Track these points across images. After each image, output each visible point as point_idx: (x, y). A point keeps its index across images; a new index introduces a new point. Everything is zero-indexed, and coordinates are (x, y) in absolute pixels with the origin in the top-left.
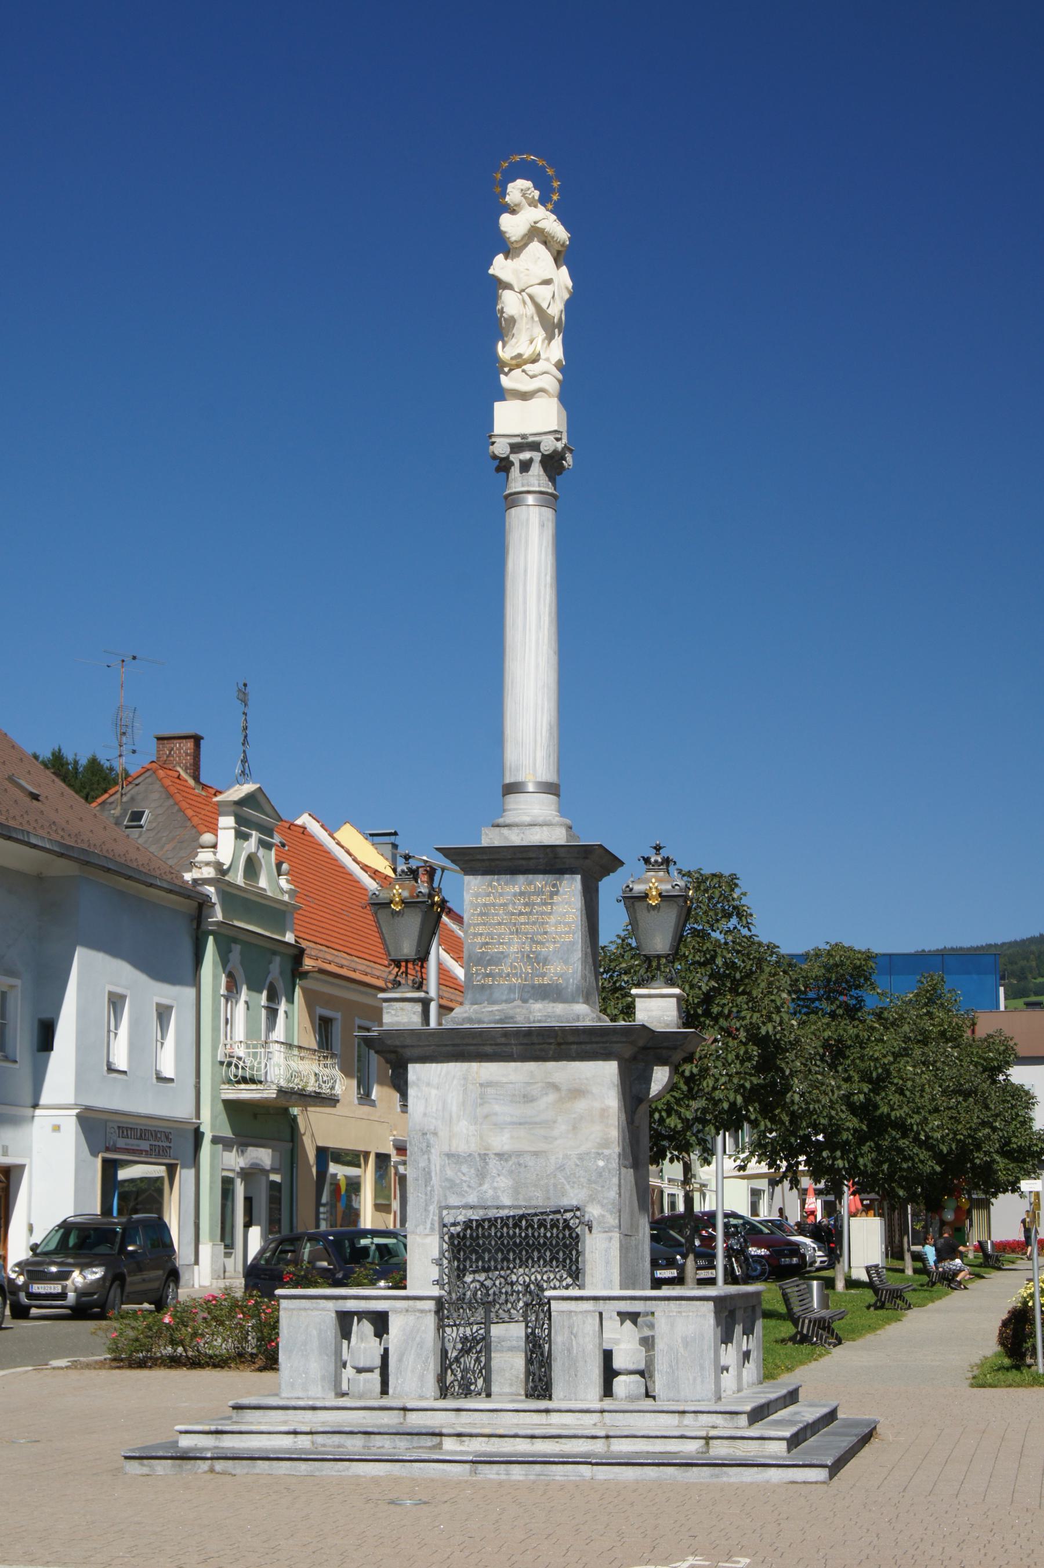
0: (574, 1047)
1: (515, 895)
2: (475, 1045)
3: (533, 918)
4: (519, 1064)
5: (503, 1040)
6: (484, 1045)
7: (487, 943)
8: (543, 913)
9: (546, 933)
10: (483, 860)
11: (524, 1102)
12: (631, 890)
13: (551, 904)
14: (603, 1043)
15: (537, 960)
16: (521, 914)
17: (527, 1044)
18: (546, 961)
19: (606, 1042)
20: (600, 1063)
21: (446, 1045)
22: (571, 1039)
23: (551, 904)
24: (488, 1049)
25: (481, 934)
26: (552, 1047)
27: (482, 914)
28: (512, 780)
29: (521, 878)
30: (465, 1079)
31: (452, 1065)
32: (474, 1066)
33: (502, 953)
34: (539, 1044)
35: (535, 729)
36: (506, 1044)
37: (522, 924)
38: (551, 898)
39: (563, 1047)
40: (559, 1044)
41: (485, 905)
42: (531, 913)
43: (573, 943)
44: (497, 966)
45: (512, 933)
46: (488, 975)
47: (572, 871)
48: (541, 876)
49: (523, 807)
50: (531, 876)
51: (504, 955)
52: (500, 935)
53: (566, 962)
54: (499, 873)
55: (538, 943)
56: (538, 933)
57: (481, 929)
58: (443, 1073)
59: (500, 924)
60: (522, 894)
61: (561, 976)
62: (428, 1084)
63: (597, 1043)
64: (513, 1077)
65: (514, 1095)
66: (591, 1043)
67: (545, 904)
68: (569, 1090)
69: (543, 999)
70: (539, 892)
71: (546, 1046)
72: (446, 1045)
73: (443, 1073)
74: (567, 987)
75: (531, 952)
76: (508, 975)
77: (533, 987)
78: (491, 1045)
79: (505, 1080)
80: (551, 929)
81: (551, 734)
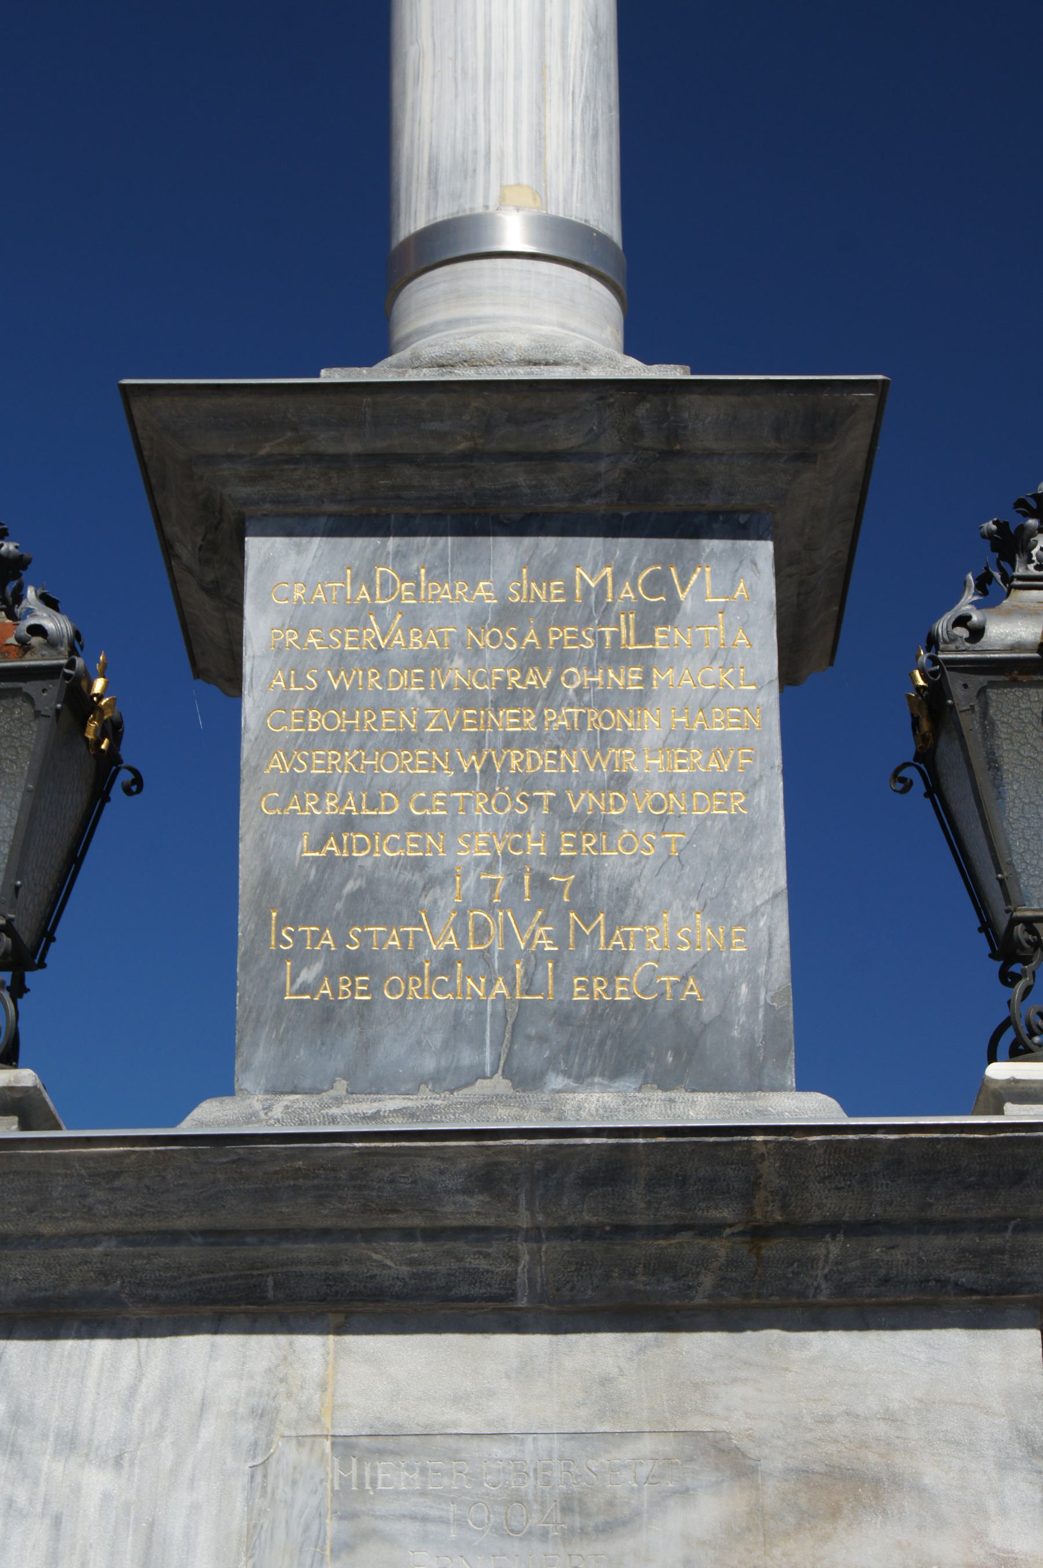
0: (833, 1248)
1: (477, 620)
2: (324, 1234)
3: (558, 719)
4: (539, 1343)
5: (473, 1208)
6: (369, 1235)
7: (349, 823)
8: (604, 698)
9: (621, 781)
10: (340, 462)
11: (569, 1535)
12: (977, 633)
13: (638, 657)
14: (983, 1226)
15: (578, 897)
16: (507, 697)
17: (588, 1233)
18: (622, 905)
19: (998, 1225)
20: (955, 1341)
21: (175, 1237)
22: (825, 1202)
23: (638, 657)
24: (388, 1261)
25: (321, 785)
26: (720, 1248)
27: (326, 699)
28: (442, 213)
29: (507, 552)
30: (263, 1415)
31: (194, 1346)
32: (312, 1347)
33: (419, 864)
34: (656, 1231)
35: (541, 24)
36: (483, 1233)
37: (509, 741)
38: (645, 634)
39: (774, 1249)
40: (758, 1233)
41: (341, 660)
42: (551, 696)
43: (747, 828)
44: (391, 919)
45: (465, 781)
46: (353, 965)
47: (736, 525)
48: (593, 545)
49: (487, 311)
50: (549, 544)
51: (425, 875)
52: (403, 789)
53: (717, 909)
54: (407, 528)
55: (587, 822)
56: (585, 783)
57: (322, 761)
58: (147, 1391)
59: (406, 740)
60: (507, 614)
61: (697, 969)
62: (69, 1443)
63: (953, 1226)
64: (508, 1409)
65: (517, 1499)
66: (926, 1226)
67: (618, 657)
68: (803, 1474)
69: (615, 1073)
70: (598, 608)
71: (690, 1245)
72: (175, 1237)
73: (147, 1391)
74: (722, 1020)
75: (554, 858)
76: (447, 962)
77: (565, 1016)
78: (408, 1234)
79: (467, 1422)
80: (644, 763)
81: (596, 55)
